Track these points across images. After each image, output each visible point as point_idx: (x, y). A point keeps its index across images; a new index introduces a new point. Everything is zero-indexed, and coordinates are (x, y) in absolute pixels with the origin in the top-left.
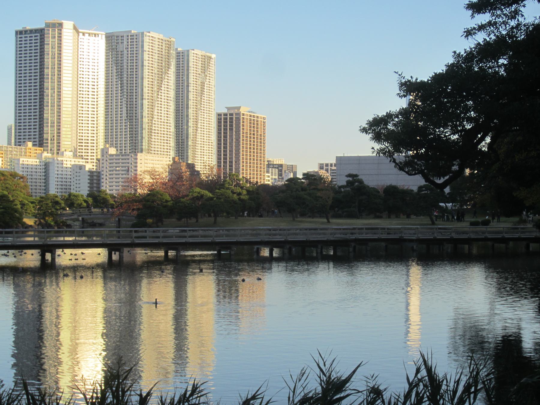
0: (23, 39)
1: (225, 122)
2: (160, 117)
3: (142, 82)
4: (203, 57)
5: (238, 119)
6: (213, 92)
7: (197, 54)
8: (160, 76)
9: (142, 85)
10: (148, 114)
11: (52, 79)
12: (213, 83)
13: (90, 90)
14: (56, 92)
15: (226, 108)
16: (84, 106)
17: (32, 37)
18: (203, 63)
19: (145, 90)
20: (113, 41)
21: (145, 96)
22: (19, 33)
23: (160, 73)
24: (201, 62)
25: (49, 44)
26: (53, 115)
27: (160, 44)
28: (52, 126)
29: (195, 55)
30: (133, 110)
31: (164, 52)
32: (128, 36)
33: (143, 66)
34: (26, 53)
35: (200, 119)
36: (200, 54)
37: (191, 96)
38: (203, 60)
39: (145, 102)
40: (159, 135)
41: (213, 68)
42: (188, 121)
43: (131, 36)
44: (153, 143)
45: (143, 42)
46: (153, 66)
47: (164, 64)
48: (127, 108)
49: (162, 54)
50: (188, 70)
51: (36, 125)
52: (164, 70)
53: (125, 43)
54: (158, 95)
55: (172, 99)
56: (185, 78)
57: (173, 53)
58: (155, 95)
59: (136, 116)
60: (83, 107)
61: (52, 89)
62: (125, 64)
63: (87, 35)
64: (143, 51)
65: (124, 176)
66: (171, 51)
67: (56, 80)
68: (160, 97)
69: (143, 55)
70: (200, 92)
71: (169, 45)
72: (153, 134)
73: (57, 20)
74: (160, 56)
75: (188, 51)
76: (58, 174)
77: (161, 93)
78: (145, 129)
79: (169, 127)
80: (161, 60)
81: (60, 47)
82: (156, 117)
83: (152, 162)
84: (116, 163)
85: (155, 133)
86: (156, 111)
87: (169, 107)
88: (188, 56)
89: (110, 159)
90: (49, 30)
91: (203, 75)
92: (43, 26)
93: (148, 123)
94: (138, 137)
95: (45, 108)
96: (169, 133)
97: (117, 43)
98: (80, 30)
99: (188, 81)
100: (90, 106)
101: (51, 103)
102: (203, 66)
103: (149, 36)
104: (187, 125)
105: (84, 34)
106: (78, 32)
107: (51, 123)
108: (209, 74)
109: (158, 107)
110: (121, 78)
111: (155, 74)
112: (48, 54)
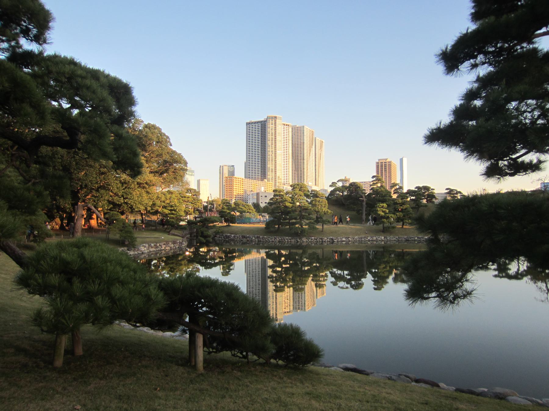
5: (390, 165)
22: (247, 124)
39: (305, 161)
45: (303, 130)
64: (304, 135)
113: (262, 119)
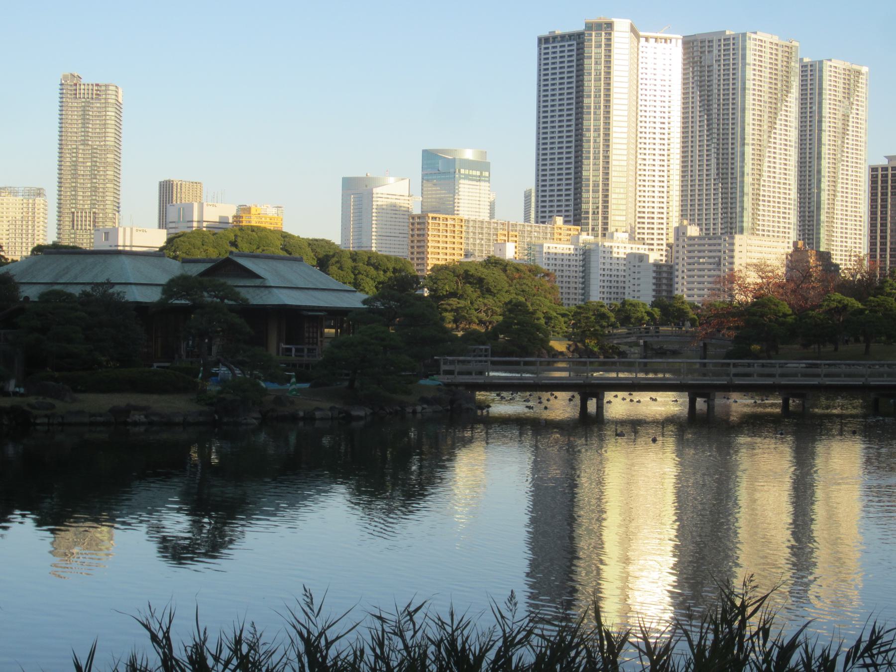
0: (550, 51)
1: (885, 181)
2: (772, 175)
3: (743, 117)
4: (847, 72)
6: (863, 131)
7: (836, 67)
8: (774, 106)
9: (743, 122)
10: (753, 169)
11: (595, 113)
12: (863, 114)
13: (658, 131)
14: (602, 135)
15: (886, 157)
16: (647, 157)
17: (564, 46)
18: (847, 82)
19: (749, 130)
20: (695, 49)
21: (749, 139)
22: (544, 41)
23: (774, 101)
24: (842, 81)
25: (590, 57)
26: (596, 173)
27: (774, 52)
28: (596, 191)
29: (833, 69)
30: (727, 164)
31: (780, 66)
32: (720, 40)
33: (744, 89)
34: (555, 74)
35: (841, 176)
36: (842, 67)
37: (825, 138)
38: (847, 77)
39: (748, 150)
40: (771, 204)
41: (863, 90)
42: (819, 181)
43: (725, 40)
44: (760, 218)
45: (744, 49)
46: (762, 89)
47: (779, 85)
48: (718, 159)
49: (776, 69)
50: (820, 94)
51: (569, 190)
52: (779, 95)
53: (715, 52)
54: (770, 137)
55: (793, 144)
56: (815, 108)
57: (796, 66)
58: (765, 137)
59: (732, 174)
60: (645, 159)
61: (595, 131)
62: (715, 86)
63: (652, 41)
64: (744, 64)
65: (712, 273)
66: (793, 64)
67: (602, 116)
68: (772, 140)
69: (744, 71)
70: (841, 131)
71: (789, 53)
72: (761, 203)
73: (603, 18)
74: (774, 72)
75: (821, 62)
76: (604, 270)
77: (775, 133)
78: (748, 194)
79: (787, 192)
80: (776, 79)
81: (608, 62)
82: (765, 174)
83: (759, 249)
84: (699, 251)
85: (764, 201)
86: (766, 164)
87: (788, 158)
88: (821, 70)
89: (690, 245)
90: (591, 35)
91: (847, 103)
92: (579, 27)
93: (753, 184)
94: (736, 208)
95: (585, 162)
96: (787, 201)
97: (701, 52)
98: (641, 34)
99: (820, 112)
100: (657, 157)
101: (595, 153)
102: (847, 86)
103: (755, 40)
104: (819, 188)
105: (647, 39)
106: (638, 37)
107: (594, 186)
108: (857, 100)
109: (769, 157)
110: (708, 110)
111: (765, 102)
112: (590, 74)
113: (577, 26)
